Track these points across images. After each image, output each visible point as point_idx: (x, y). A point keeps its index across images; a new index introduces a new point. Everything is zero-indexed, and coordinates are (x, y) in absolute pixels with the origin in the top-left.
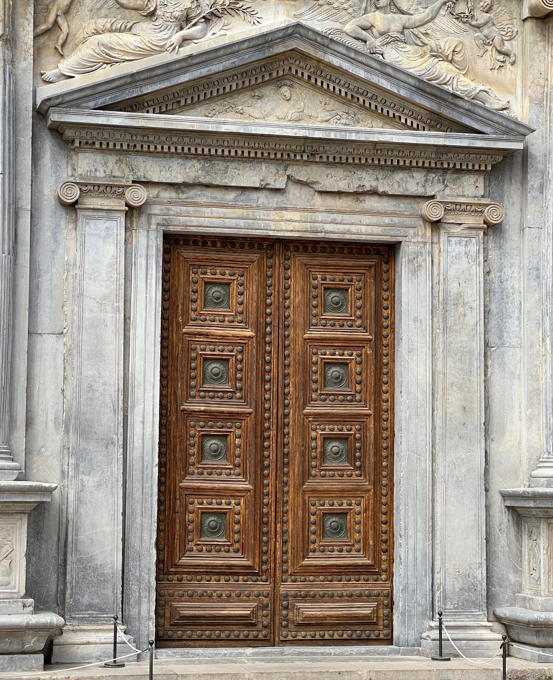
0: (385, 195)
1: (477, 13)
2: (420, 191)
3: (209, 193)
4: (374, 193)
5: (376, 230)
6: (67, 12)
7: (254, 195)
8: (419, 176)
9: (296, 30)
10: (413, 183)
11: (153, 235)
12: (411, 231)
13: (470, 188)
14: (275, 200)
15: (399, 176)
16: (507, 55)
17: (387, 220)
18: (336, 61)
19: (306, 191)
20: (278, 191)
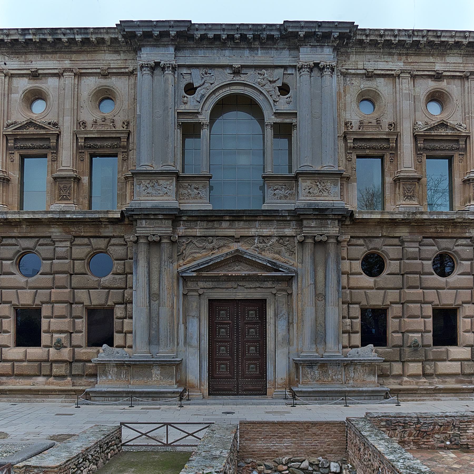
0: (262, 287)
1: (285, 242)
2: (271, 286)
3: (219, 289)
4: (260, 287)
5: (260, 296)
6: (185, 250)
7: (230, 289)
8: (270, 282)
9: (237, 251)
10: (269, 284)
11: (206, 301)
12: (269, 296)
13: (283, 285)
14: (234, 291)
15: (266, 283)
16: (293, 252)
17: (263, 294)
18: (247, 257)
19: (242, 287)
20: (235, 288)
